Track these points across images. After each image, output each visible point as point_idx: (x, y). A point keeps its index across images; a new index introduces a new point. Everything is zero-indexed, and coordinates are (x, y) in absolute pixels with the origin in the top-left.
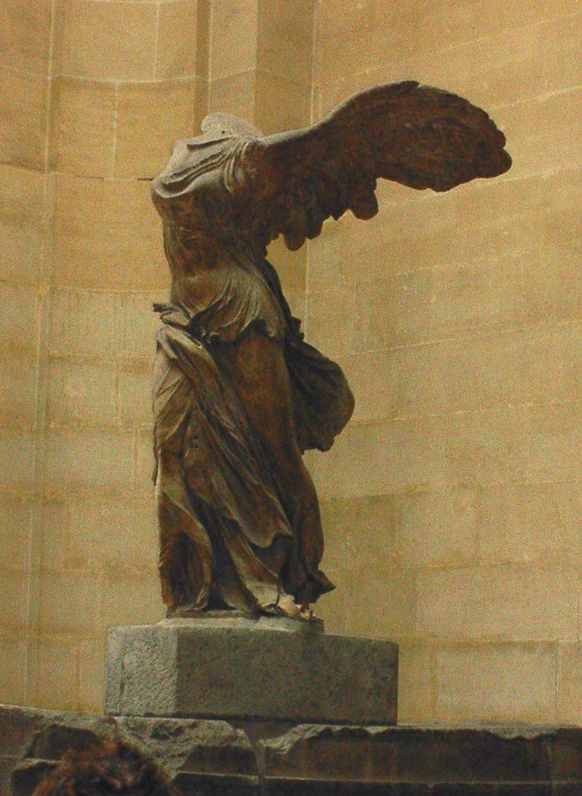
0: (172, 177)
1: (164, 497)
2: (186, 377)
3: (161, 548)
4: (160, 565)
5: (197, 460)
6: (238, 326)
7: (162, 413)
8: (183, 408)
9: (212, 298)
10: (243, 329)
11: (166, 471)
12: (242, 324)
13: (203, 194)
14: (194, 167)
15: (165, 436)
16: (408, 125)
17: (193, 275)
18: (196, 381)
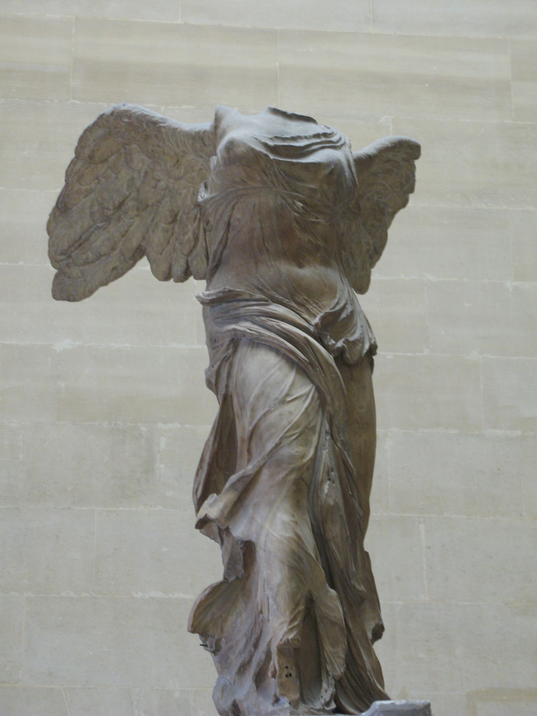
0: (271, 139)
1: (299, 540)
2: (318, 389)
3: (291, 613)
4: (291, 636)
5: (335, 500)
6: (361, 345)
7: (296, 425)
8: (315, 426)
9: (336, 300)
10: (365, 351)
11: (297, 505)
12: (363, 344)
13: (333, 171)
14: (306, 138)
15: (303, 457)
16: (375, 198)
17: (301, 266)
18: (329, 399)
